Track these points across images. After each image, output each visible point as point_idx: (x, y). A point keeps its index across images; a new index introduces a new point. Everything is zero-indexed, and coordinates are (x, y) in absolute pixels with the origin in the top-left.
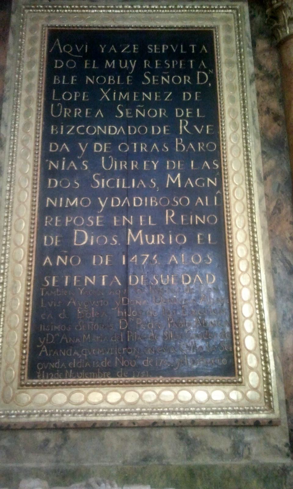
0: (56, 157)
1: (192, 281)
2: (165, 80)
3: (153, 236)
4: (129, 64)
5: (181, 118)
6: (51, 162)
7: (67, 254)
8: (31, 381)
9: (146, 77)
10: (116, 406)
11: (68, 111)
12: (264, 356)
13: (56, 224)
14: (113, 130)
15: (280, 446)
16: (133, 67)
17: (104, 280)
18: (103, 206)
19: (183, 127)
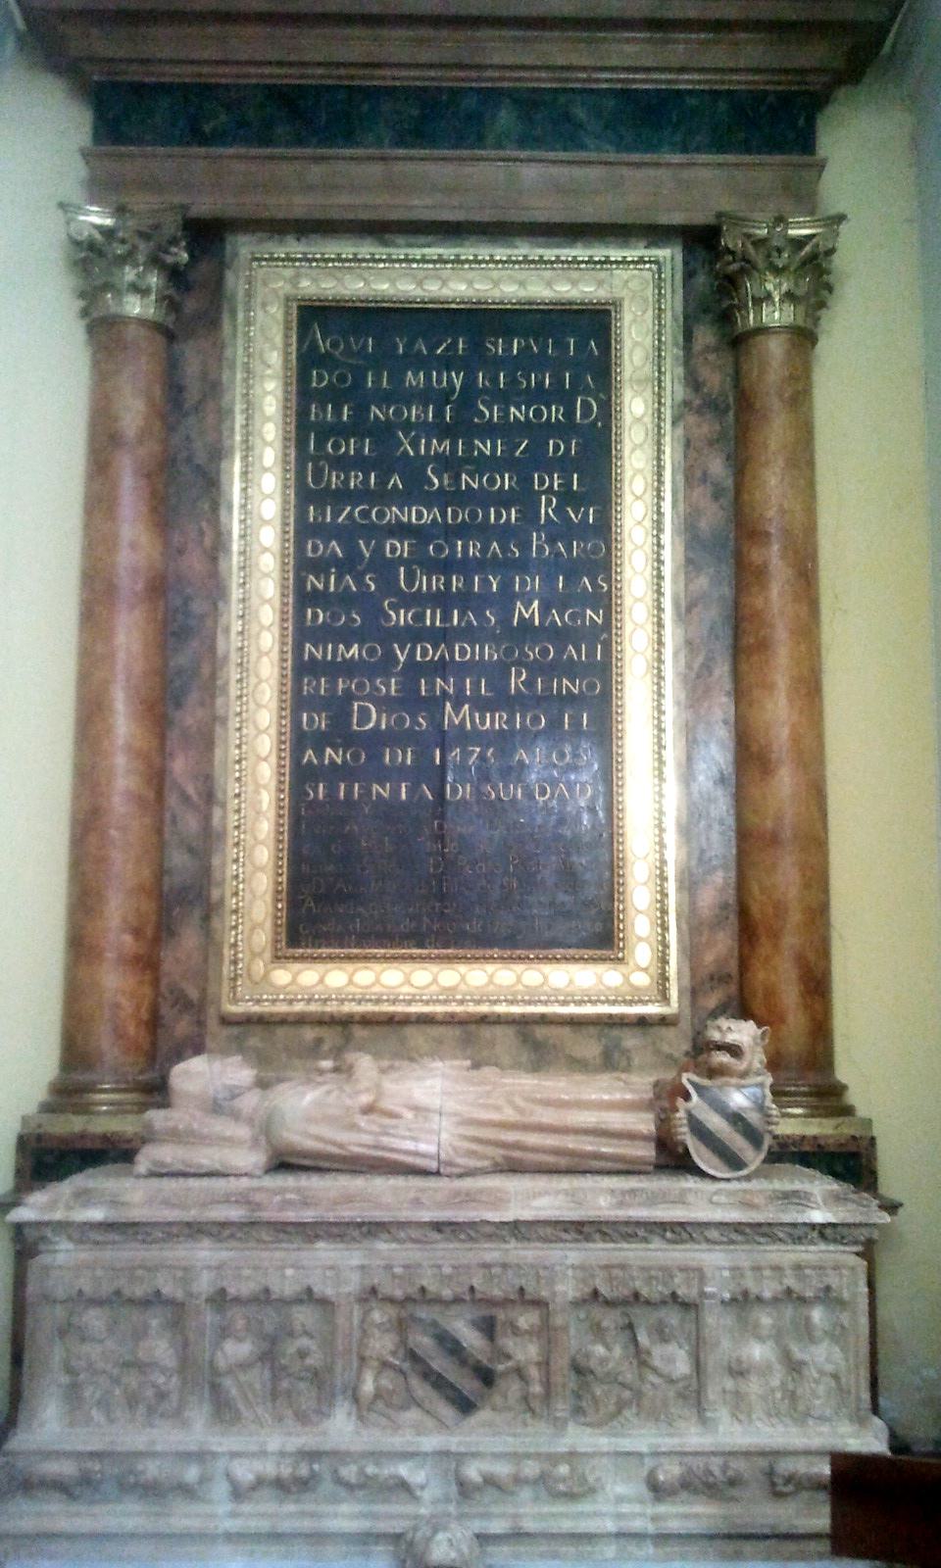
0: (319, 567)
1: (553, 795)
2: (518, 414)
3: (488, 715)
4: (449, 378)
5: (544, 492)
6: (311, 577)
7: (341, 745)
8: (291, 950)
9: (481, 407)
10: (426, 991)
11: (338, 477)
12: (662, 918)
13: (322, 692)
14: (420, 515)
15: (676, 1055)
16: (458, 387)
17: (404, 790)
18: (402, 659)
19: (546, 510)
